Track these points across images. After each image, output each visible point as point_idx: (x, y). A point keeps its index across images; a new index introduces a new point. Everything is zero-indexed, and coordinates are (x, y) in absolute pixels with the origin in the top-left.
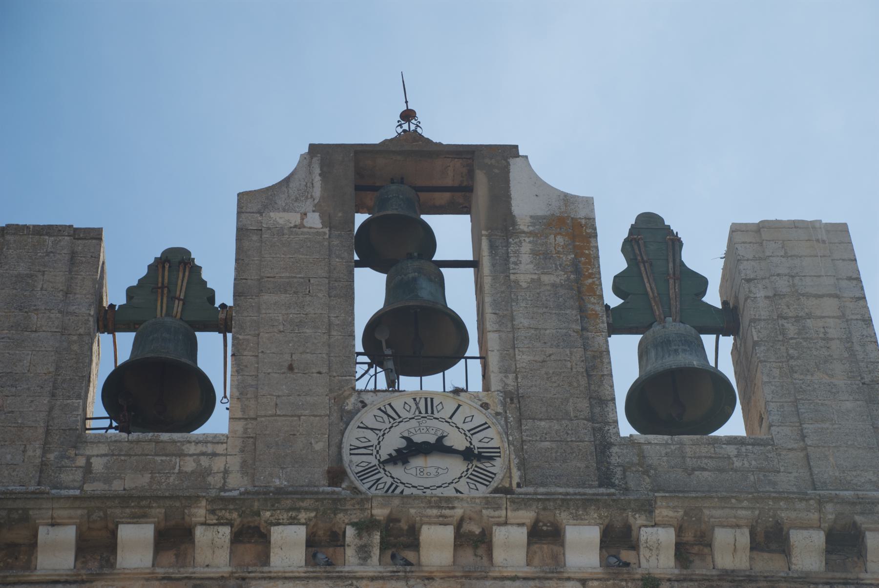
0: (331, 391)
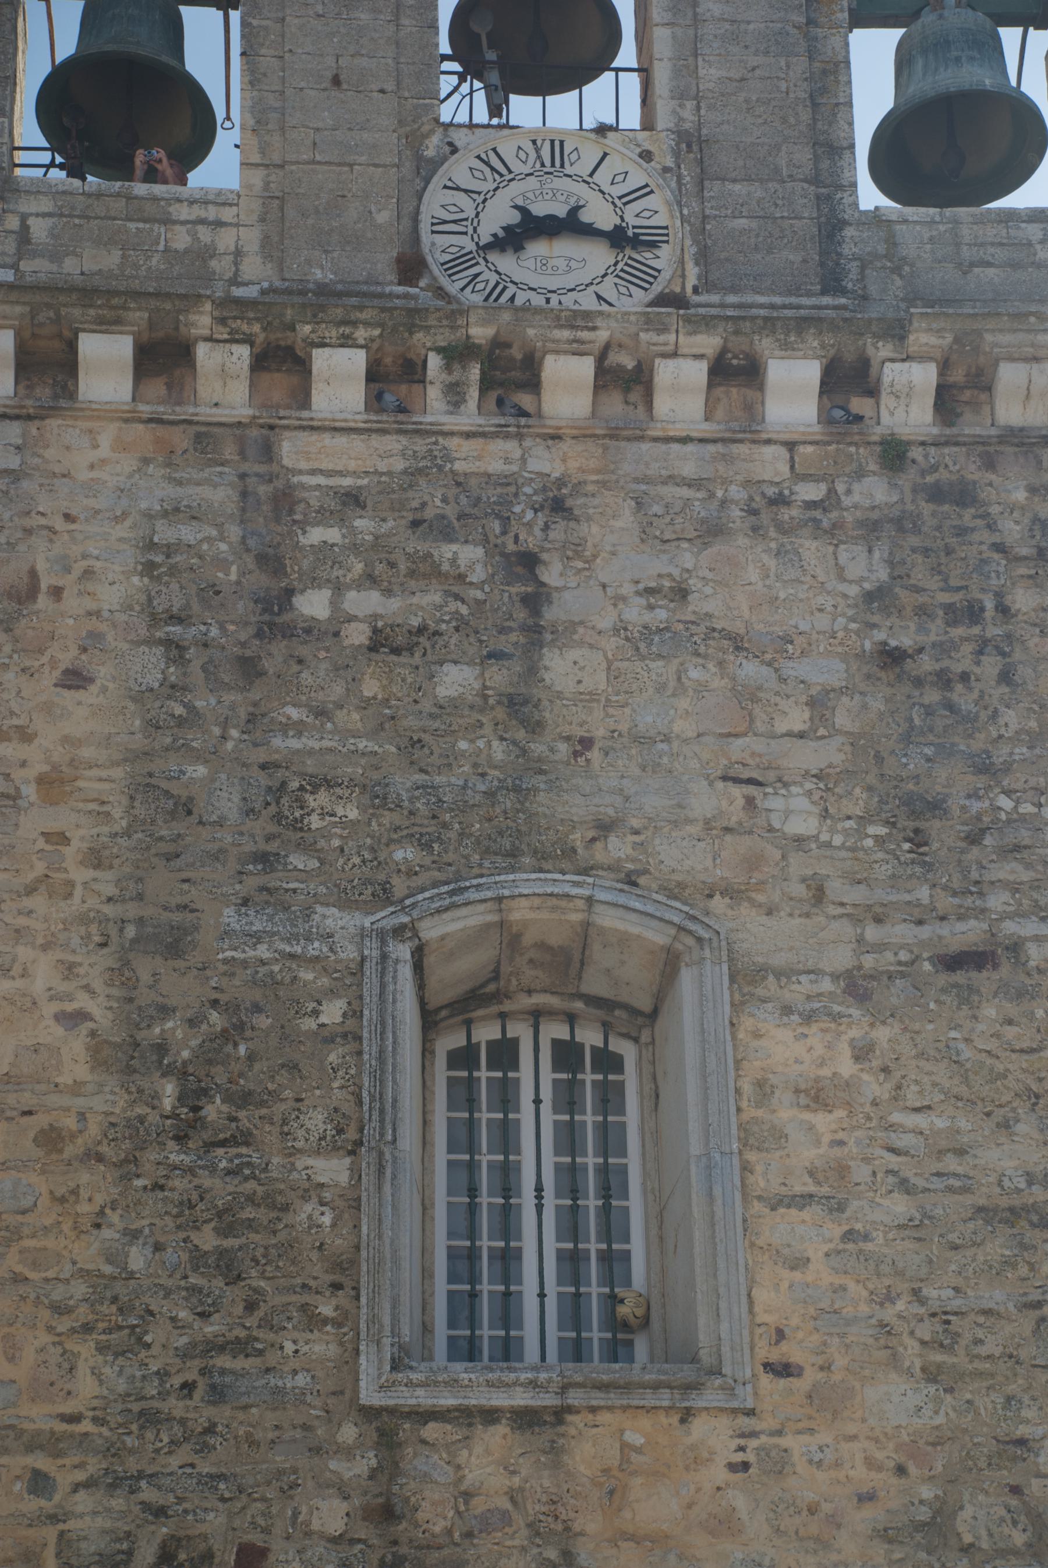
0: (401, 123)
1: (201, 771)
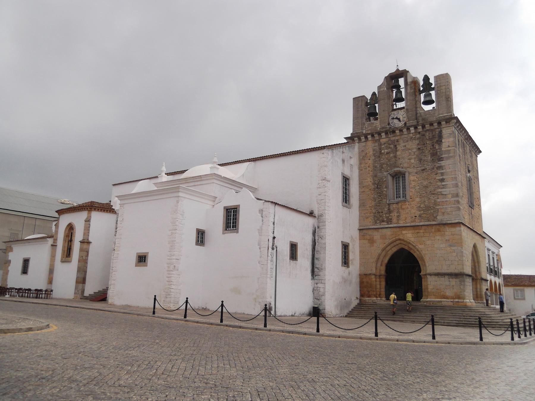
1: (377, 164)
